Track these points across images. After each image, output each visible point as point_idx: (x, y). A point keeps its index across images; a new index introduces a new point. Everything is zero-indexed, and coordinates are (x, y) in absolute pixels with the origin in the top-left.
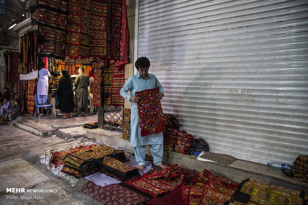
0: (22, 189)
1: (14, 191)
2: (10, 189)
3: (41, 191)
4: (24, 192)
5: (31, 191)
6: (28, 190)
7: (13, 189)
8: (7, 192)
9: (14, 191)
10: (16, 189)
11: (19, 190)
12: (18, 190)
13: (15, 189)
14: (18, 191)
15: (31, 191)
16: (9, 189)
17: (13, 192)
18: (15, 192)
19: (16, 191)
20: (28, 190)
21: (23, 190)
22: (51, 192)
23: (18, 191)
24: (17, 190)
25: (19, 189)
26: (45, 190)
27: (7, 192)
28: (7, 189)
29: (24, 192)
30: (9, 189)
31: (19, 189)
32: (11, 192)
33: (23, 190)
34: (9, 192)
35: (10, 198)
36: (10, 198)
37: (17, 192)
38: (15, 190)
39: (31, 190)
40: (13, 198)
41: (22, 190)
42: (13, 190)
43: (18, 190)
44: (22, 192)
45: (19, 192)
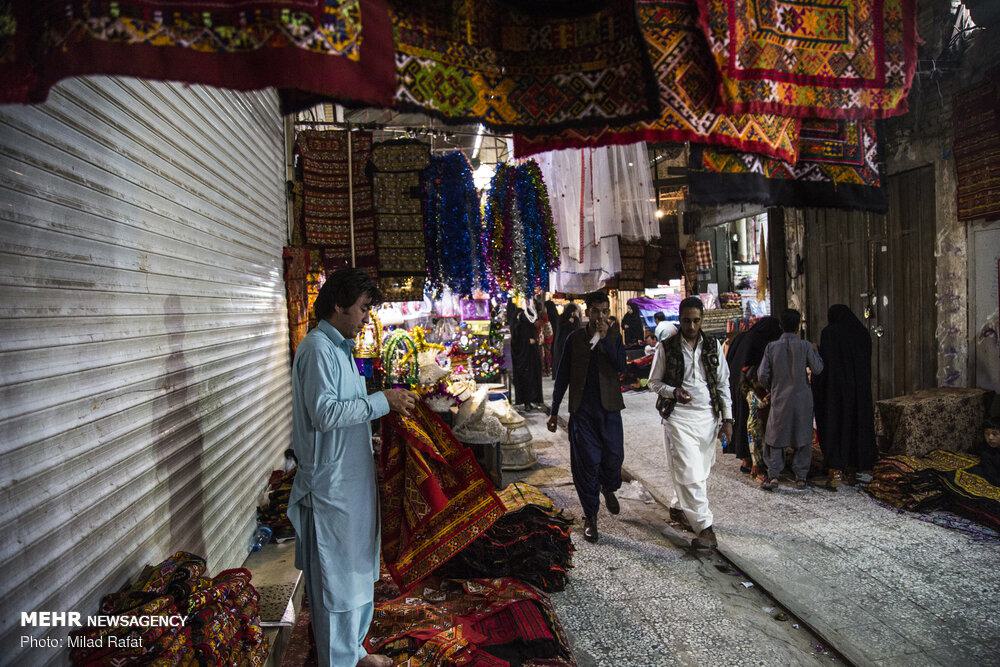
0: (71, 614)
1: (45, 621)
2: (34, 614)
3: (132, 622)
4: (79, 624)
5: (100, 621)
6: (90, 618)
7: (42, 614)
8: (23, 624)
9: (45, 621)
10: (51, 616)
11: (63, 619)
12: (59, 619)
13: (49, 613)
14: (59, 622)
15: (102, 623)
16: (29, 614)
17: (42, 624)
18: (48, 625)
19: (50, 621)
20: (90, 618)
21: (74, 617)
22: (166, 625)
23: (59, 622)
24: (55, 618)
25: (63, 614)
26: (144, 619)
27: (23, 624)
28: (24, 615)
29: (79, 624)
30: (29, 614)
31: (63, 614)
32: (34, 624)
33: (74, 617)
34: (29, 625)
35: (34, 642)
36: (34, 642)
37: (55, 624)
38: (48, 619)
39: (102, 618)
40: (42, 643)
41: (71, 620)
42: (42, 619)
43: (59, 619)
44: (70, 624)
45: (63, 624)
